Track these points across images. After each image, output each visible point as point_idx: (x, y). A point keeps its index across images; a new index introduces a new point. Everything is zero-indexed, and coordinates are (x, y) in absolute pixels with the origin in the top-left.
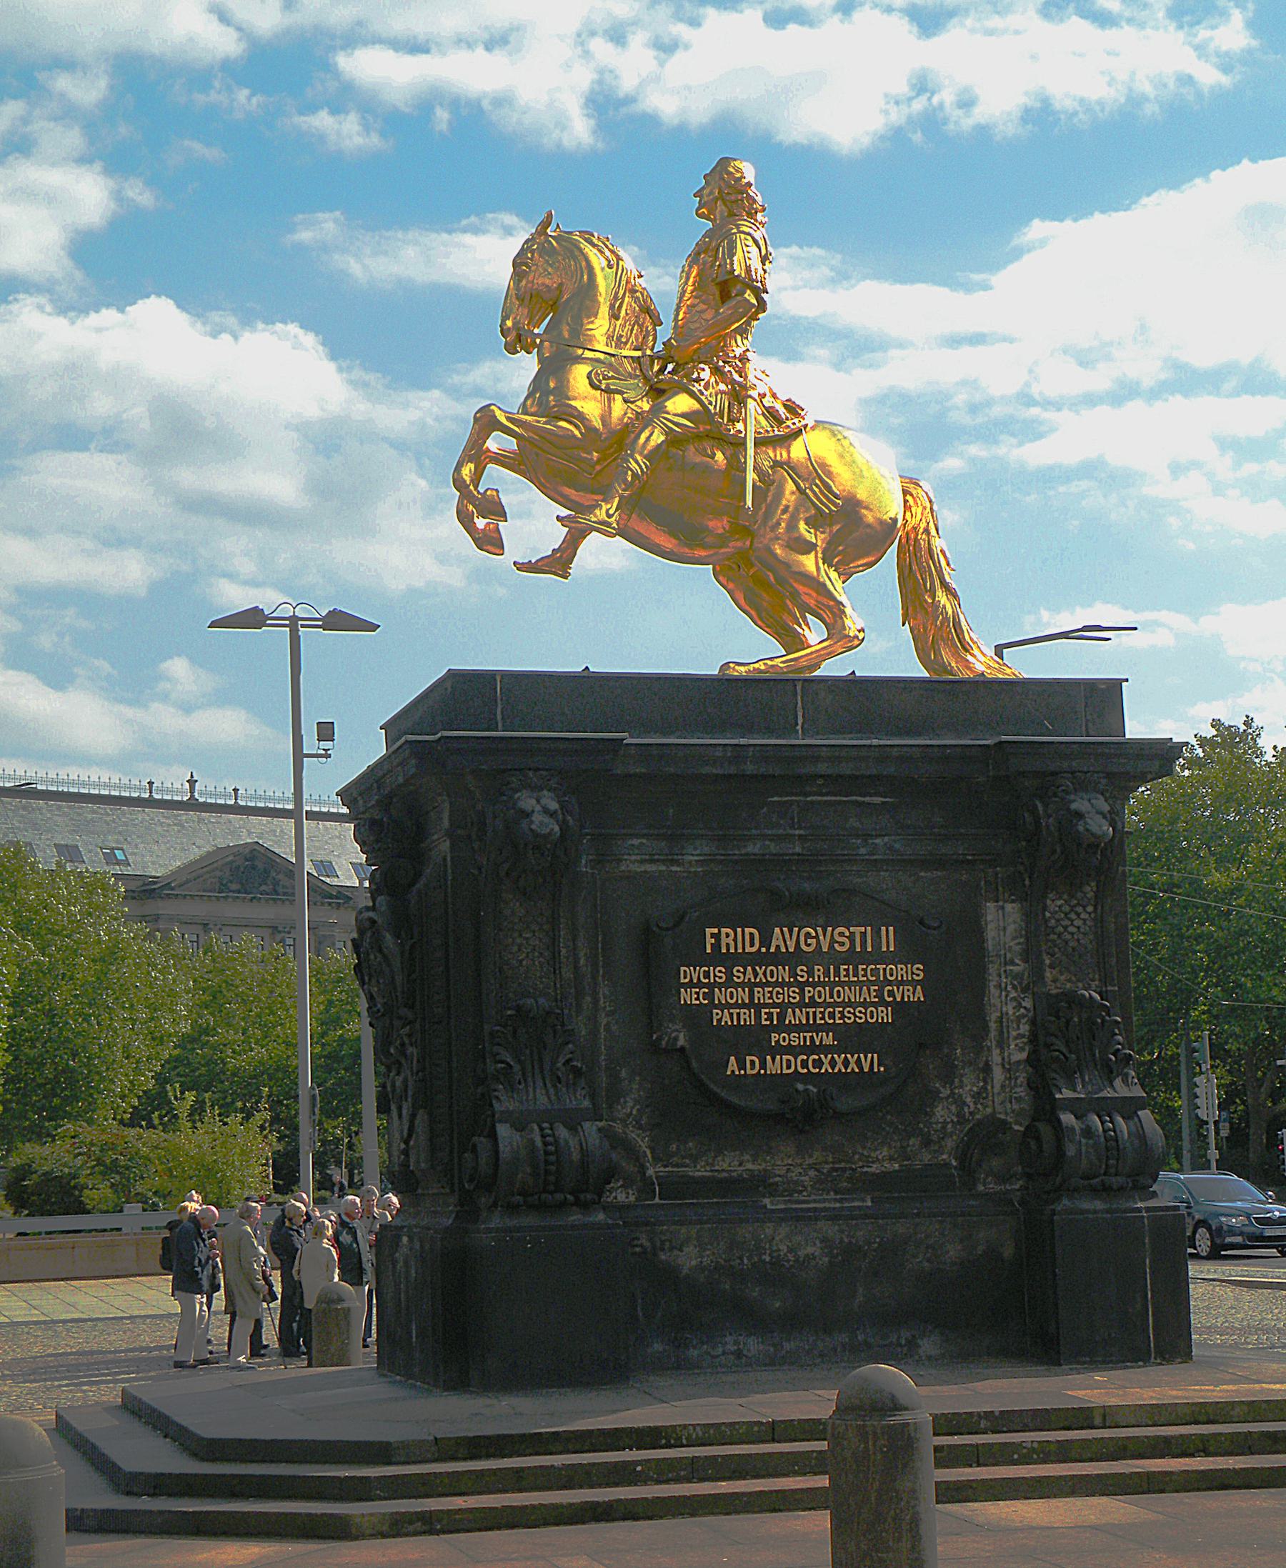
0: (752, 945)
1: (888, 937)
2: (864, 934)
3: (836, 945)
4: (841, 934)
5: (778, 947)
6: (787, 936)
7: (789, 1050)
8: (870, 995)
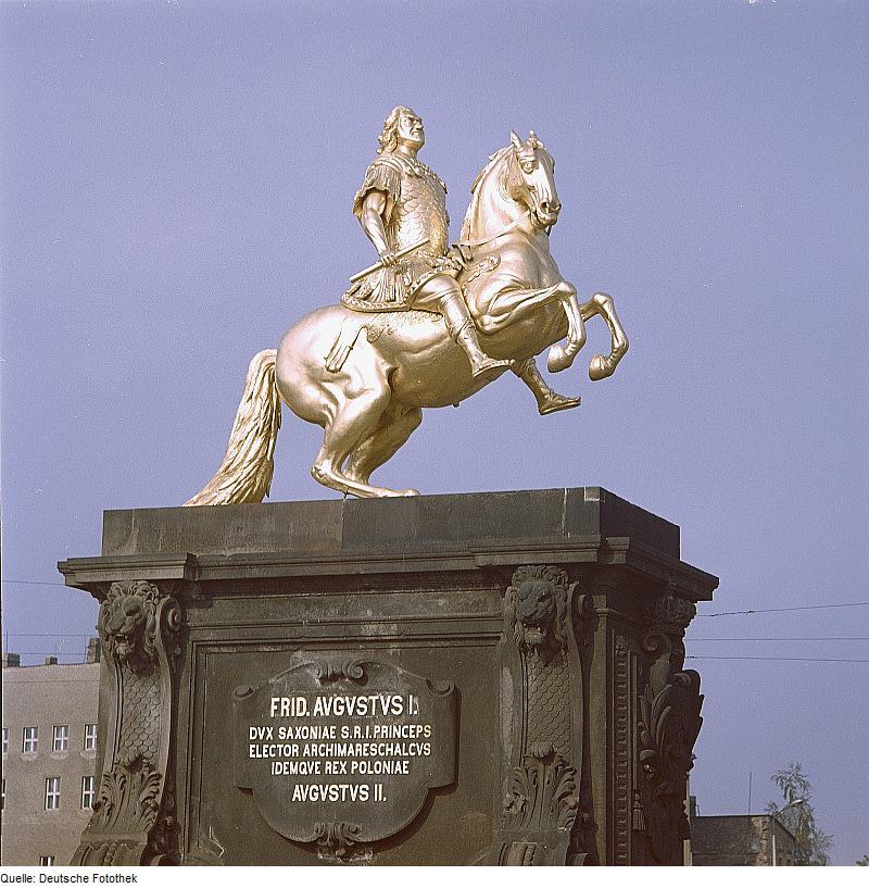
0: (301, 710)
2: (378, 701)
3: (358, 710)
4: (362, 702)
5: (319, 712)
6: (325, 705)
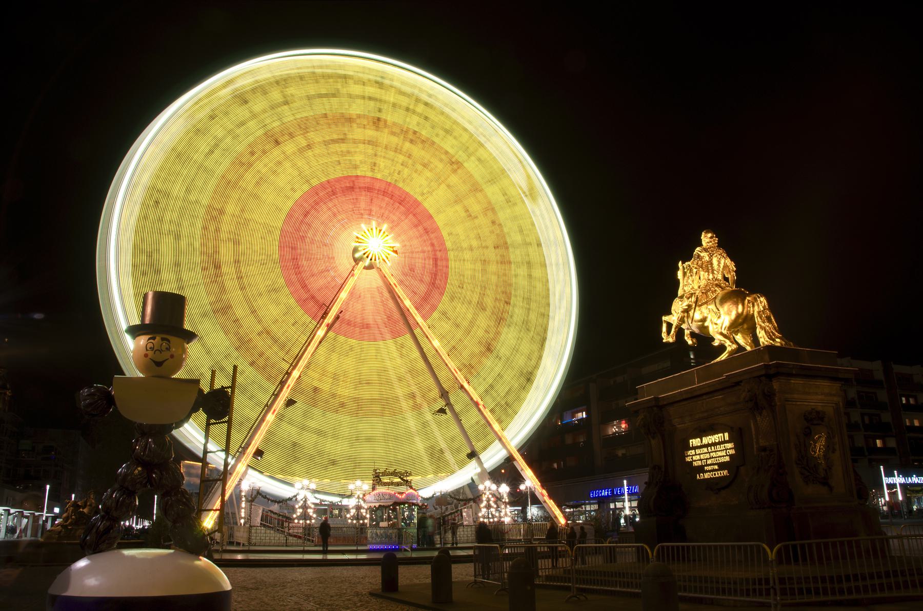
1: (726, 435)
7: (710, 471)
8: (724, 453)
